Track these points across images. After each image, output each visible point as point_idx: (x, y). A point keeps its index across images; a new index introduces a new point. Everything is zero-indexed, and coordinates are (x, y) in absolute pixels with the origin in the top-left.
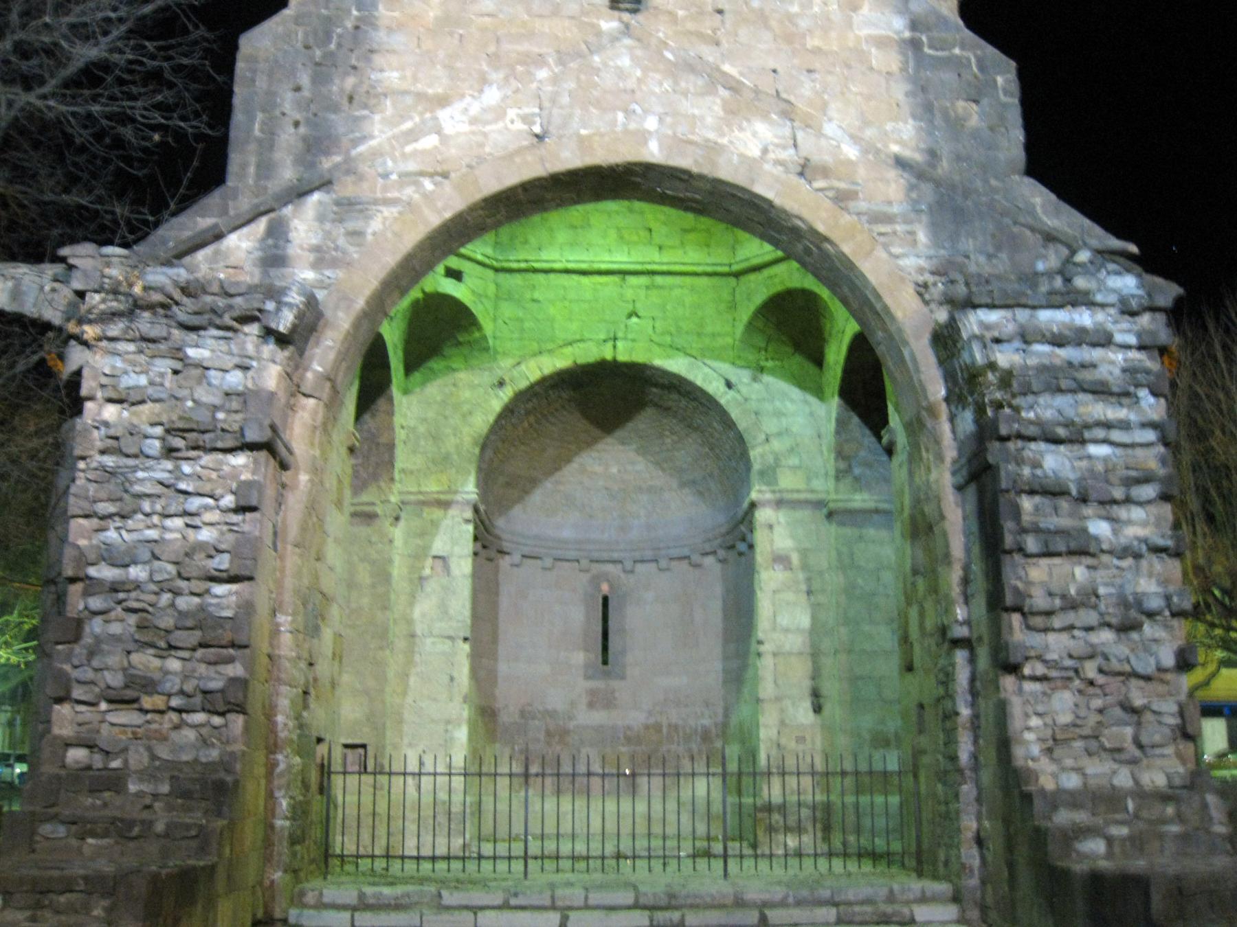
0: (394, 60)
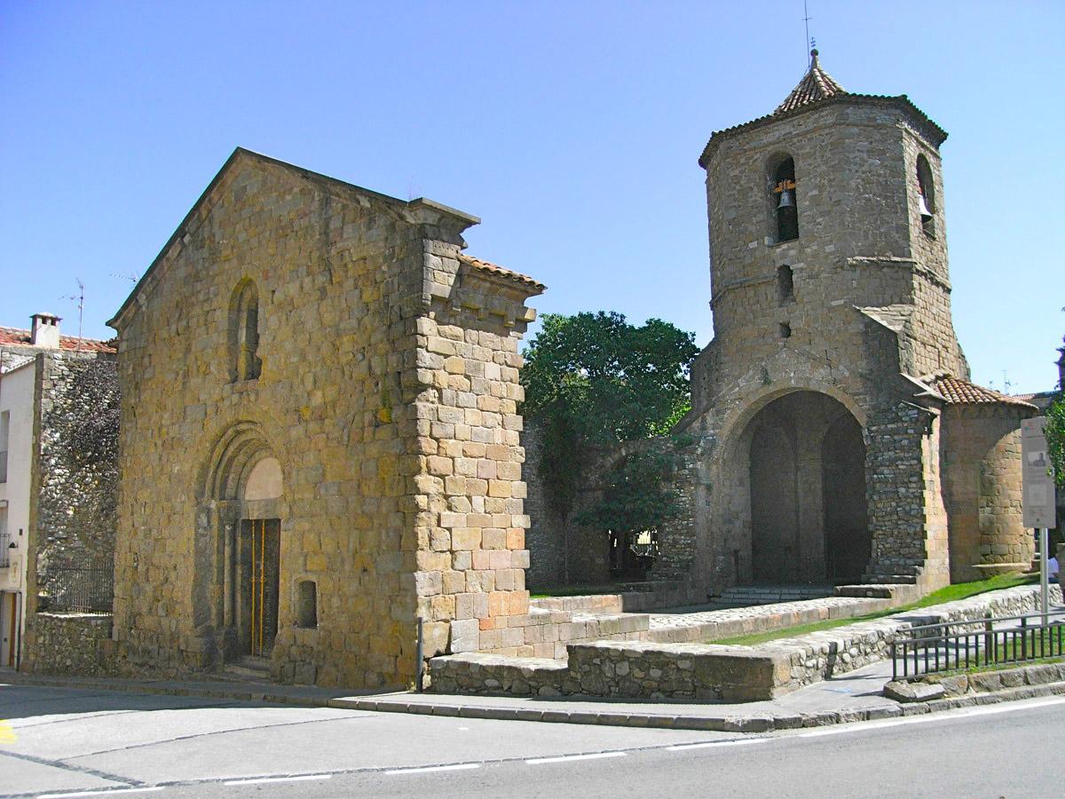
0: (727, 366)
